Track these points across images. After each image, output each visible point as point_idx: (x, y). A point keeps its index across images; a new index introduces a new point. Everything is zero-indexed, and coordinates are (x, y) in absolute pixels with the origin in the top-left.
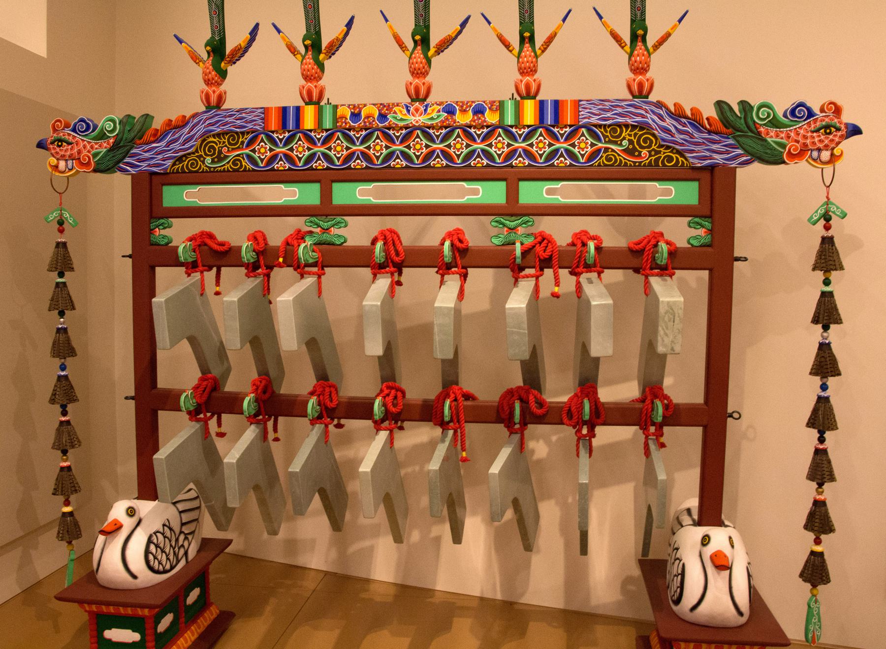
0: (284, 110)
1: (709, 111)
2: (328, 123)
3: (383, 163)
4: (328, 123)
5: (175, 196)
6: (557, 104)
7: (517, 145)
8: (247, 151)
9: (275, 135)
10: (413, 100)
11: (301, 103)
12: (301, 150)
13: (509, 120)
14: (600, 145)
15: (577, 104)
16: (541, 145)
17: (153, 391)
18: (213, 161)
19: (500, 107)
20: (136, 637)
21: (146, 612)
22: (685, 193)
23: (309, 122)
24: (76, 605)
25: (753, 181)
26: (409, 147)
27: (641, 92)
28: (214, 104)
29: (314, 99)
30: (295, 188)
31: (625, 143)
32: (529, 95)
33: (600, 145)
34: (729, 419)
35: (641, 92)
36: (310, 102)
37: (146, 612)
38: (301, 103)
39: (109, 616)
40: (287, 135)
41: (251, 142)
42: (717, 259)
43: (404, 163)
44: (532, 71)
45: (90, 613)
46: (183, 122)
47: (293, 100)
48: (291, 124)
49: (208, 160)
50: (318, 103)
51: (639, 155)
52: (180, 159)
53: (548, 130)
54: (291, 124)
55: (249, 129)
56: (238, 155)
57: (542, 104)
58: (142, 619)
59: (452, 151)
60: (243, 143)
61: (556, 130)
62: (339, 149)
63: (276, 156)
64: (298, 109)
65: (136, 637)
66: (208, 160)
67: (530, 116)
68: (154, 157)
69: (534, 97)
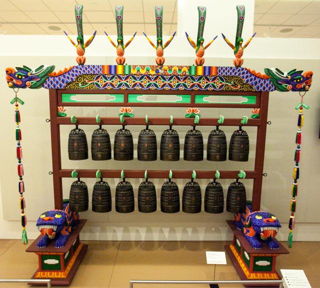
0: (110, 67)
1: (263, 73)
2: (127, 73)
3: (147, 87)
4: (127, 73)
5: (66, 98)
6: (210, 68)
7: (212, 83)
8: (96, 82)
9: (107, 76)
10: (158, 65)
11: (116, 64)
12: (116, 82)
13: (193, 73)
14: (224, 83)
15: (217, 68)
16: (203, 83)
17: (60, 171)
18: (82, 85)
19: (190, 68)
20: (57, 262)
21: (61, 254)
22: (252, 100)
23: (120, 71)
24: (34, 253)
25: (275, 96)
26: (156, 82)
27: (238, 65)
28: (81, 63)
29: (122, 62)
30: (113, 96)
31: (232, 82)
32: (201, 65)
33: (224, 83)
34: (263, 176)
35: (238, 65)
36: (121, 64)
37: (61, 254)
38: (117, 64)
39: (45, 255)
40: (111, 76)
41: (97, 78)
42: (261, 122)
43: (155, 88)
44: (241, 54)
45: (39, 255)
46: (71, 69)
47: (114, 63)
48: (113, 72)
49: (80, 85)
50: (123, 64)
51: (237, 87)
52: (68, 84)
53: (206, 77)
54: (113, 72)
55: (96, 73)
56: (91, 84)
57: (205, 68)
58: (59, 255)
59: (201, 84)
60: (94, 78)
61: (208, 77)
62: (131, 82)
63: (107, 84)
64: (116, 67)
65: (57, 262)
66: (80, 85)
67: (200, 72)
68: (60, 84)
69: (201, 65)
